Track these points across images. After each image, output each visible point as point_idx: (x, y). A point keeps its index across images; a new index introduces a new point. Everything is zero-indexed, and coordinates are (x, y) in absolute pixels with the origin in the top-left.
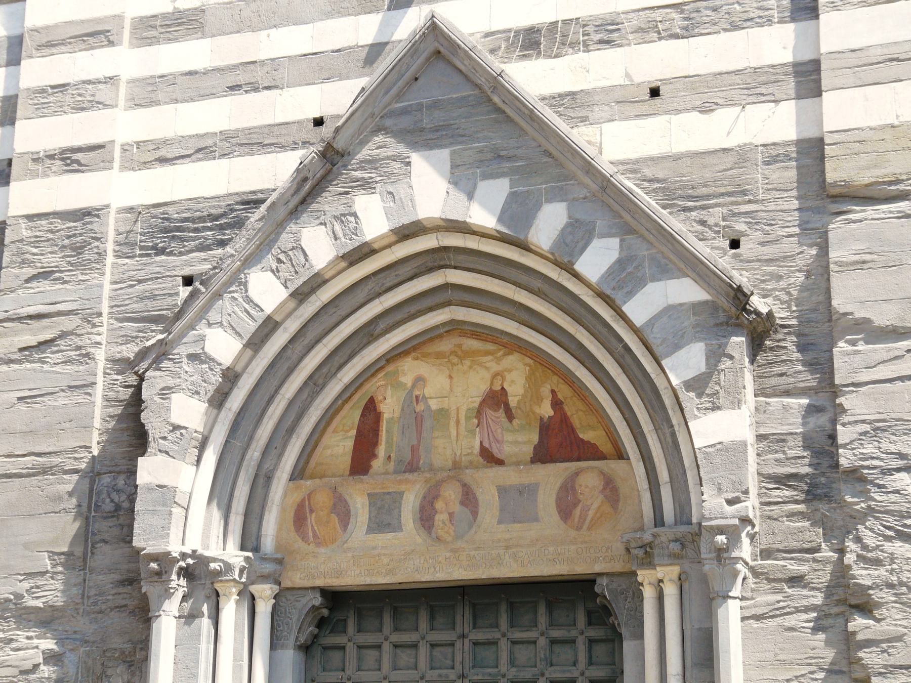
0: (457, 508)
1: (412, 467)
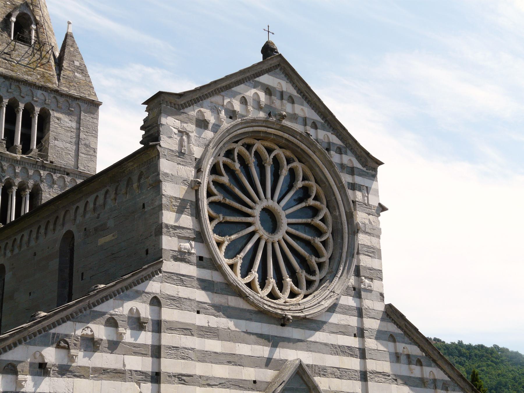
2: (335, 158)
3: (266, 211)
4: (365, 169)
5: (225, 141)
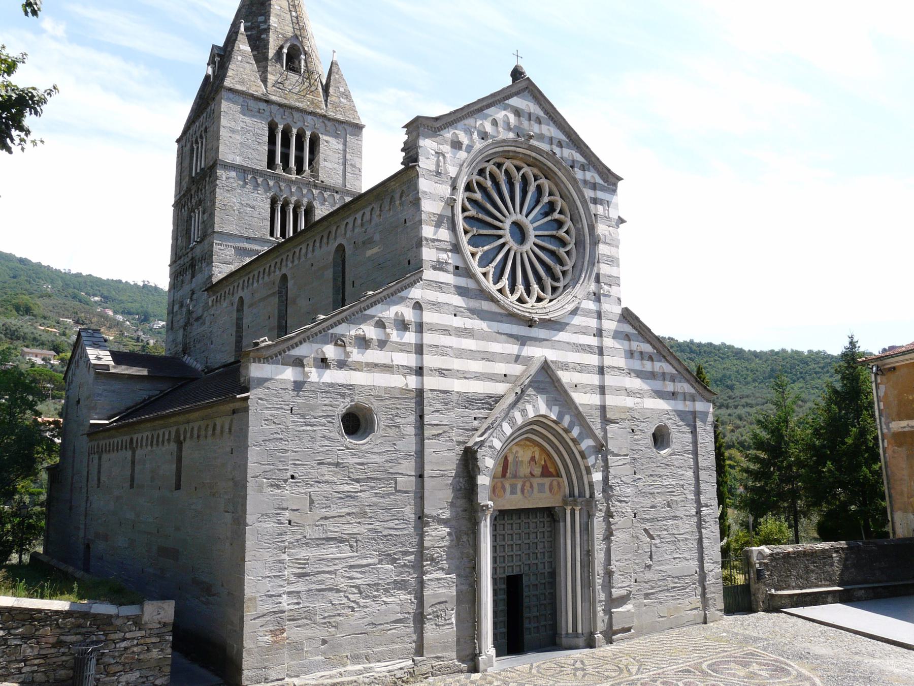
0: (529, 488)
1: (515, 476)
2: (579, 174)
3: (515, 224)
4: (606, 185)
5: (477, 160)
